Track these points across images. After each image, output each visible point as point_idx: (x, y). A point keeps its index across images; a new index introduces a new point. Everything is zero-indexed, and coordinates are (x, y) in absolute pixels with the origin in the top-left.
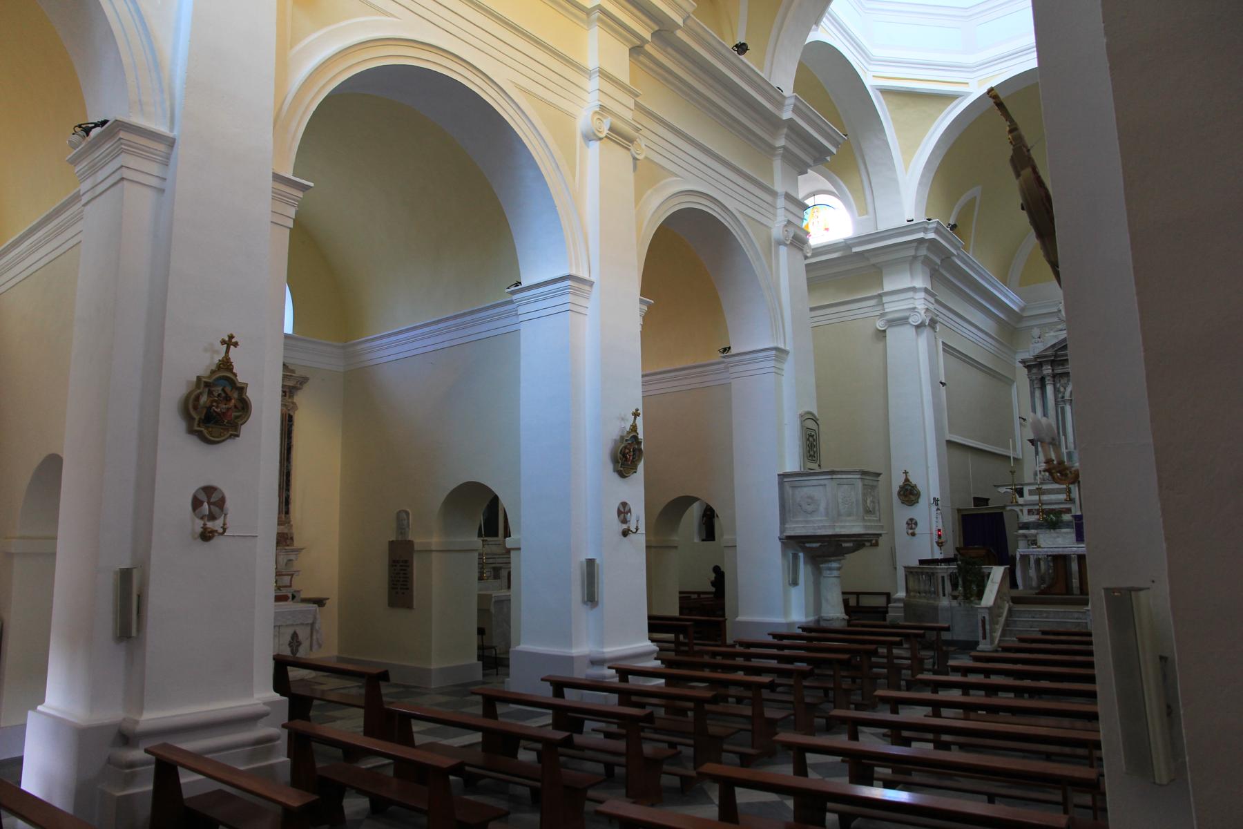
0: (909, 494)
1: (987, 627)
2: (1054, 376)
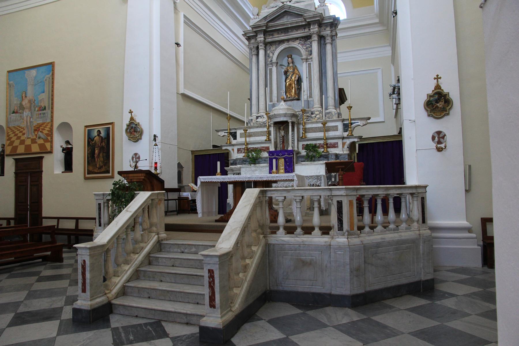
0: (134, 131)
1: (88, 275)
2: (266, 44)
